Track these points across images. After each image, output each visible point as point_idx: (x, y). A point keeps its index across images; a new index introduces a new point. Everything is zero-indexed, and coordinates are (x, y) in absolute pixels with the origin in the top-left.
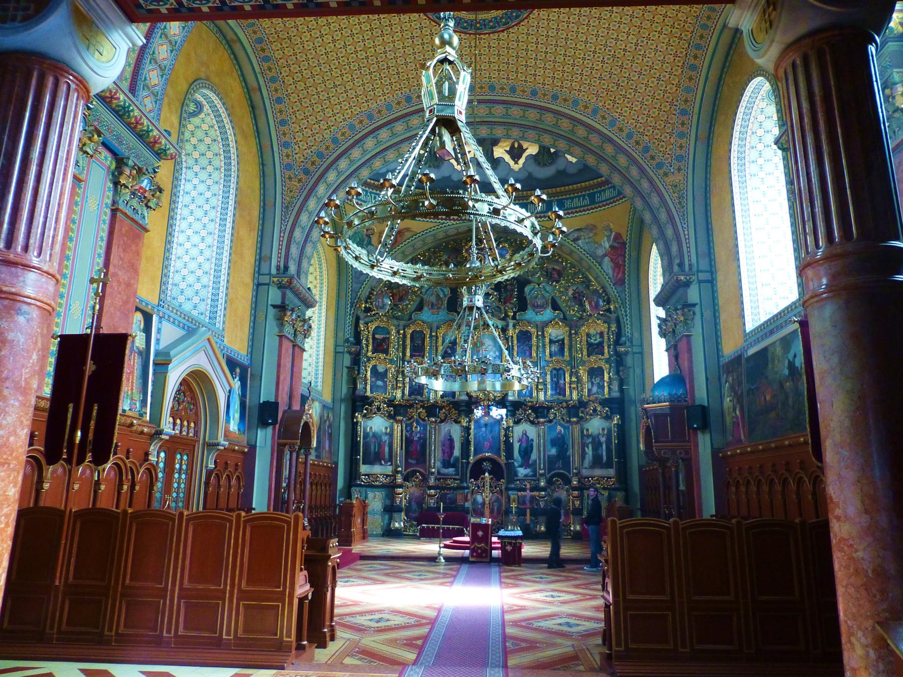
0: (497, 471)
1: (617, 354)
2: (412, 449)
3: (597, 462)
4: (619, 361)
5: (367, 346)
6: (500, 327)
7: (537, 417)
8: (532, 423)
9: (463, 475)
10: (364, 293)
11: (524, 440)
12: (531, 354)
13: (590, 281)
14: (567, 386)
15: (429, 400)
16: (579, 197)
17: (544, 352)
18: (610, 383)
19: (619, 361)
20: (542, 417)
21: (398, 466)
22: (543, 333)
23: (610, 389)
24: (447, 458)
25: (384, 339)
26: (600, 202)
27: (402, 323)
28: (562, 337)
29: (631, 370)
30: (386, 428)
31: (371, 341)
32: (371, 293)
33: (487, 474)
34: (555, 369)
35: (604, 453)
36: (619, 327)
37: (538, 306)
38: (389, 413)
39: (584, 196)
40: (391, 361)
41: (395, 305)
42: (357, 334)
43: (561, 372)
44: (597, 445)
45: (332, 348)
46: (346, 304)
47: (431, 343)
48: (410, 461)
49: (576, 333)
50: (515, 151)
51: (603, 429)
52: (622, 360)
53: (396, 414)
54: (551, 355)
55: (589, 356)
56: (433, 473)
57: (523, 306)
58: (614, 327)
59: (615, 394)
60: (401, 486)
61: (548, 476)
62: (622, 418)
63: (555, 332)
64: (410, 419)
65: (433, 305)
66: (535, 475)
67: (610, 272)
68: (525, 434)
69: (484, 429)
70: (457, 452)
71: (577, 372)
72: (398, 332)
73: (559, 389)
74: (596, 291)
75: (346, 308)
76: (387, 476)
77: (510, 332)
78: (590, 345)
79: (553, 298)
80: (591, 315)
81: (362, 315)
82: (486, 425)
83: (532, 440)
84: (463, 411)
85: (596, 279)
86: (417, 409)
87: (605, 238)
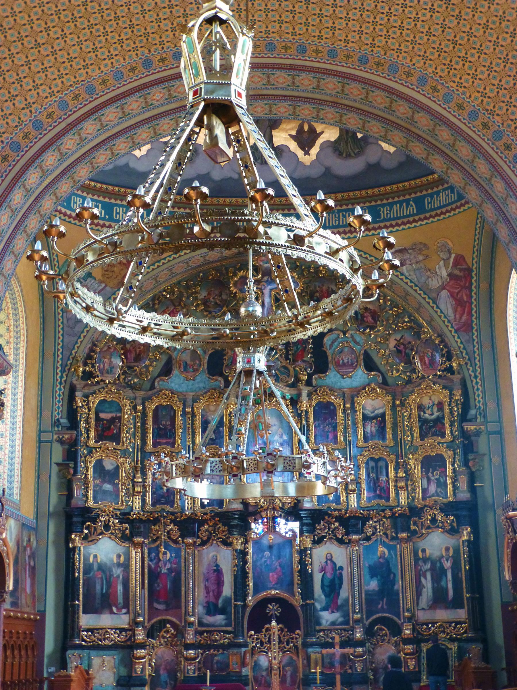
0: (289, 618)
1: (465, 435)
2: (159, 586)
3: (439, 599)
4: (467, 445)
5: (88, 431)
6: (288, 397)
7: (347, 534)
8: (341, 541)
9: (238, 625)
10: (82, 351)
11: (329, 568)
12: (336, 437)
13: (420, 326)
14: (392, 484)
15: (183, 511)
16: (401, 203)
17: (356, 433)
19: (467, 445)
20: (357, 533)
21: (137, 615)
22: (353, 403)
23: (455, 488)
24: (212, 599)
25: (112, 420)
26: (432, 210)
27: (141, 394)
28: (381, 411)
29: (486, 459)
30: (119, 556)
31: (93, 422)
32: (92, 350)
33: (274, 623)
34: (372, 459)
35: (450, 586)
36: (465, 393)
37: (344, 365)
39: (408, 201)
40: (125, 453)
41: (130, 368)
42: (72, 414)
43: (381, 464)
44: (438, 573)
45: (33, 435)
46: (55, 368)
48: (156, 605)
49: (402, 404)
50: (305, 136)
51: (447, 549)
52: (471, 444)
53: (132, 535)
56: (191, 624)
57: (321, 365)
58: (458, 395)
59: (464, 495)
60: (142, 646)
61: (367, 623)
62: (476, 531)
63: (371, 404)
64: (155, 541)
65: (186, 365)
66: (347, 622)
67: (450, 312)
68: (330, 559)
69: (267, 553)
70: (227, 590)
71: (406, 463)
72: (135, 408)
73: (379, 490)
74: (429, 342)
75: (55, 374)
76: (122, 630)
77: (304, 404)
78: (423, 422)
79: (365, 351)
80: (423, 377)
81: (79, 384)
82: (271, 547)
83: (341, 568)
84: (236, 526)
85: (429, 323)
86: (166, 525)
87: (442, 263)
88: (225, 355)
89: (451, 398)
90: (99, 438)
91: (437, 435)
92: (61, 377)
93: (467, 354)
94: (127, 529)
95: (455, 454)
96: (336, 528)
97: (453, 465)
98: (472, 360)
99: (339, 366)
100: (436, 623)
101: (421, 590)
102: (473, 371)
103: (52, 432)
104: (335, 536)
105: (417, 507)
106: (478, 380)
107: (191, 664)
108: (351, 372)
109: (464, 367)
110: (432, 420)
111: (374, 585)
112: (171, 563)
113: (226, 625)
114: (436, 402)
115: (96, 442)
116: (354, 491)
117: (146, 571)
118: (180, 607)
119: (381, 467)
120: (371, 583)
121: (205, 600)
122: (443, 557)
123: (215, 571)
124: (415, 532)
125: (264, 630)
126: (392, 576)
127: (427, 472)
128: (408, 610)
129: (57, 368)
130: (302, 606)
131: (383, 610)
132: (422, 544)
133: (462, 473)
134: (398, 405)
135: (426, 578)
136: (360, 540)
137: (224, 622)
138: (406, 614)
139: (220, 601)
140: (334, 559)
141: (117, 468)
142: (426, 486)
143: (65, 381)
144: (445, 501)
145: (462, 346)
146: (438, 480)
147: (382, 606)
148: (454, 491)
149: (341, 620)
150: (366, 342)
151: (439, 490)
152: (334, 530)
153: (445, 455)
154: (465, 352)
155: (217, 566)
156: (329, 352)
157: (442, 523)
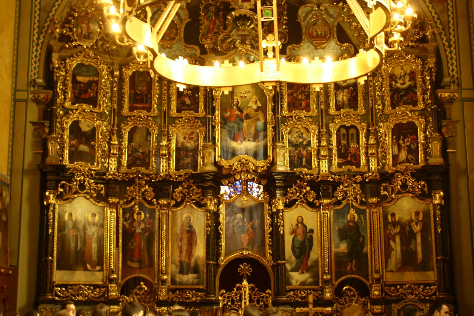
2: (134, 245)
3: (408, 260)
5: (65, 93)
7: (318, 198)
8: (311, 205)
11: (300, 231)
14: (362, 151)
18: (426, 147)
20: (327, 197)
23: (426, 154)
25: (90, 84)
29: (459, 126)
30: (94, 215)
31: (70, 84)
32: (70, 15)
33: (245, 283)
34: (343, 126)
35: (419, 249)
36: (439, 63)
37: (318, 36)
38: (98, 192)
40: (101, 116)
43: (352, 131)
44: (407, 236)
46: (31, 29)
47: (161, 89)
48: (129, 263)
51: (417, 213)
52: (444, 111)
53: (108, 195)
54: (338, 108)
55: (394, 106)
56: (164, 282)
58: (431, 62)
59: (437, 160)
61: (336, 284)
64: (128, 202)
66: (316, 283)
68: (301, 222)
69: (239, 216)
70: (200, 251)
71: (376, 132)
72: (112, 73)
73: (348, 156)
75: (31, 35)
76: (96, 286)
78: (394, 91)
81: (56, 45)
82: (243, 210)
83: (312, 231)
84: (210, 187)
86: (141, 186)
88: (201, 25)
89: (423, 67)
90: (76, 100)
91: (409, 104)
92: (38, 39)
93: (441, 24)
94: (102, 189)
95: (426, 121)
96: (307, 192)
97: (425, 132)
98: (447, 29)
100: (405, 285)
101: (390, 253)
102: (447, 41)
103: (27, 91)
105: (388, 173)
106: (452, 49)
108: (324, 43)
109: (438, 37)
110: (403, 89)
111: (343, 247)
112: (145, 223)
113: (198, 284)
114: (408, 72)
115: (73, 104)
116: (326, 156)
117: (121, 230)
119: (352, 134)
120: (341, 245)
122: (412, 221)
123: (188, 231)
124: (385, 197)
125: (235, 289)
126: (361, 239)
127: (398, 139)
128: (377, 272)
129: (34, 29)
130: (273, 267)
131: (352, 272)
132: (391, 209)
133: (434, 139)
135: (395, 242)
136: (330, 203)
137: (196, 281)
138: (375, 276)
140: (304, 222)
141: (94, 130)
142: (397, 153)
143: (42, 43)
144: (416, 167)
145: (436, 16)
146: (409, 147)
147: (351, 268)
148: (425, 157)
149: (310, 280)
150: (339, 15)
151: (410, 156)
152: (305, 194)
153: (417, 123)
154: (439, 22)
155: (190, 226)
156: (304, 24)
157: (413, 188)
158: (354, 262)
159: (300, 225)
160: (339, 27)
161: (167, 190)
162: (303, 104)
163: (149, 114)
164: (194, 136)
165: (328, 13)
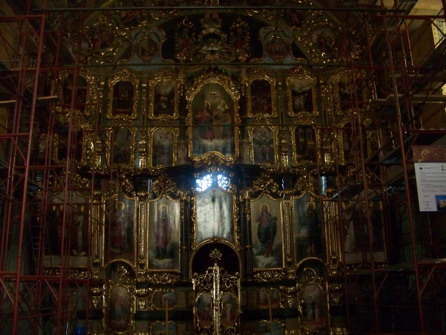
6: (230, 74)
8: (275, 195)
9: (184, 267)
22: (284, 83)
28: (307, 88)
37: (276, 53)
47: (140, 96)
57: (256, 50)
65: (143, 51)
68: (265, 210)
78: (344, 96)
86: (121, 180)
99: (271, 53)
101: (345, 237)
104: (270, 191)
107: (141, 301)
108: (281, 58)
111: (304, 232)
118: (133, 252)
119: (309, 133)
121: (155, 246)
134: (322, 84)
139: (168, 246)
147: (311, 251)
156: (264, 43)
158: (313, 245)
159: (264, 213)
160: (294, 44)
161: (145, 183)
162: (266, 107)
163: (129, 117)
164: (169, 136)
165: (284, 34)
